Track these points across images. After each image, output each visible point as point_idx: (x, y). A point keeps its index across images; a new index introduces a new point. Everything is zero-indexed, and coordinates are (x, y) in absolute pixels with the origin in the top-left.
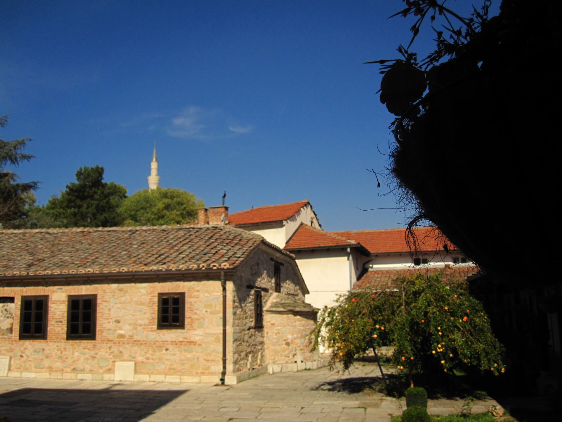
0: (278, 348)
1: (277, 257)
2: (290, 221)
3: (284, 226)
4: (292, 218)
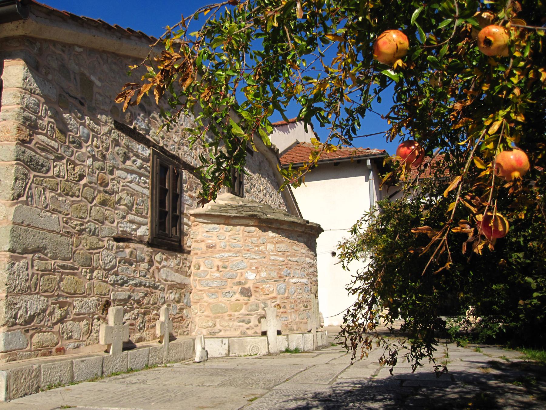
2: (278, 130)
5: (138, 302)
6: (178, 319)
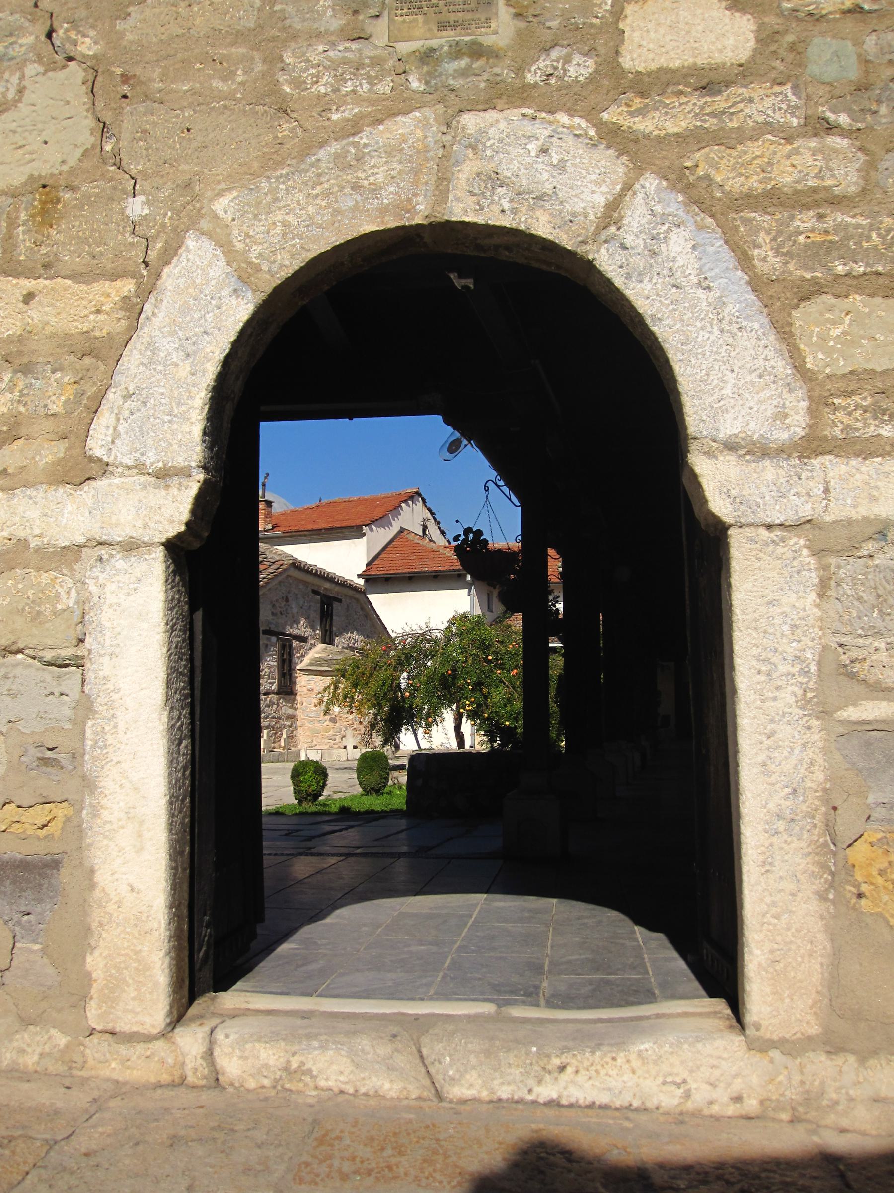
0: (318, 726)
1: (325, 589)
3: (364, 535)
4: (381, 521)
5: (273, 727)
6: (290, 737)
